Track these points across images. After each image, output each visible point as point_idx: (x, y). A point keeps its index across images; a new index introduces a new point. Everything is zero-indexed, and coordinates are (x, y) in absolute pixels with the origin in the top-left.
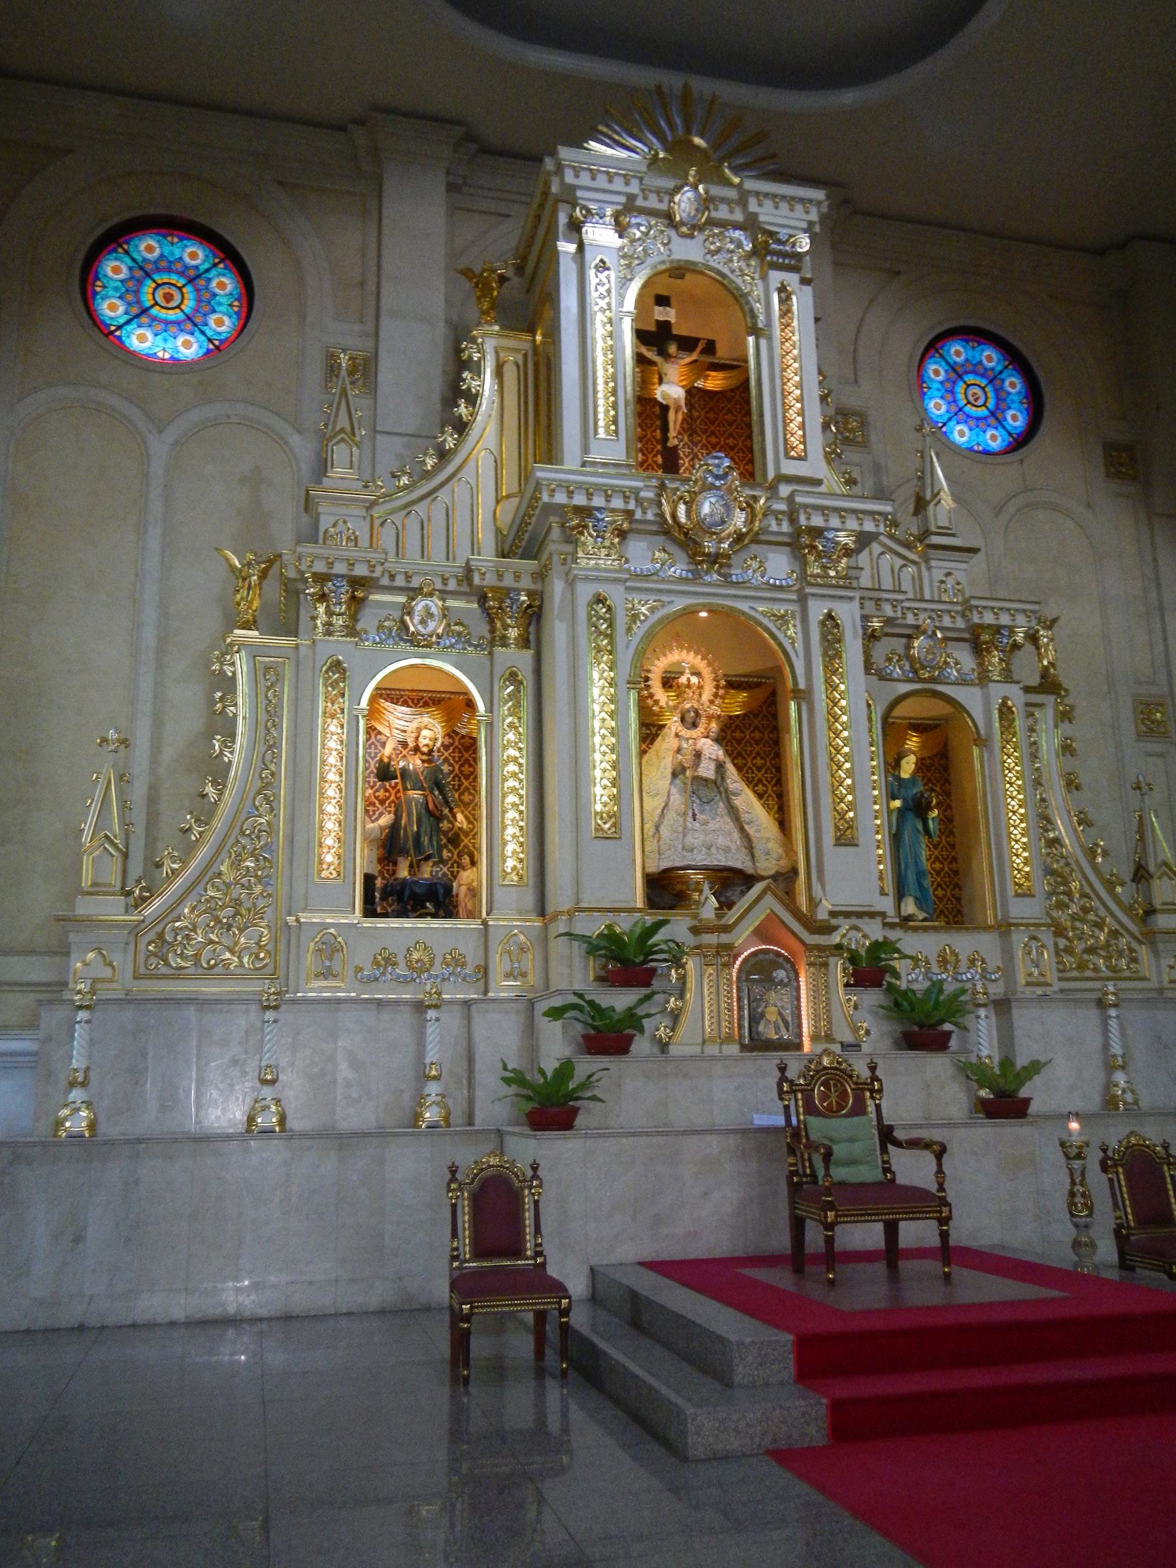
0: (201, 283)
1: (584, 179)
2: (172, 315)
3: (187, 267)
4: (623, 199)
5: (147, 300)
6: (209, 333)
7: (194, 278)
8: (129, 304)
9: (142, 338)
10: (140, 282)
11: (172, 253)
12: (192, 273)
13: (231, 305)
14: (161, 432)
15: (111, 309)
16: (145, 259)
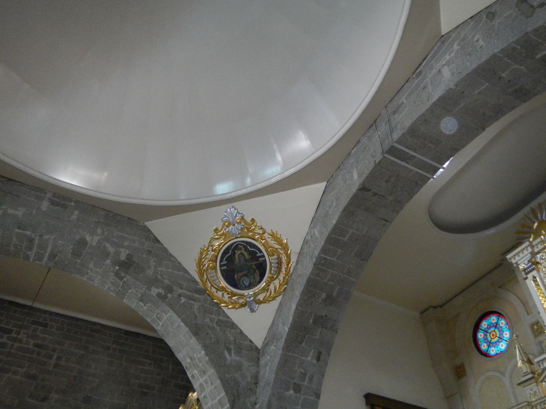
0: (498, 326)
1: (517, 258)
2: (497, 339)
3: (493, 324)
4: (529, 255)
5: (489, 339)
6: (505, 339)
7: (496, 326)
8: (487, 343)
9: (493, 351)
10: (486, 335)
11: (489, 322)
12: (495, 325)
13: (506, 328)
14: (504, 376)
15: (484, 347)
16: (485, 328)
